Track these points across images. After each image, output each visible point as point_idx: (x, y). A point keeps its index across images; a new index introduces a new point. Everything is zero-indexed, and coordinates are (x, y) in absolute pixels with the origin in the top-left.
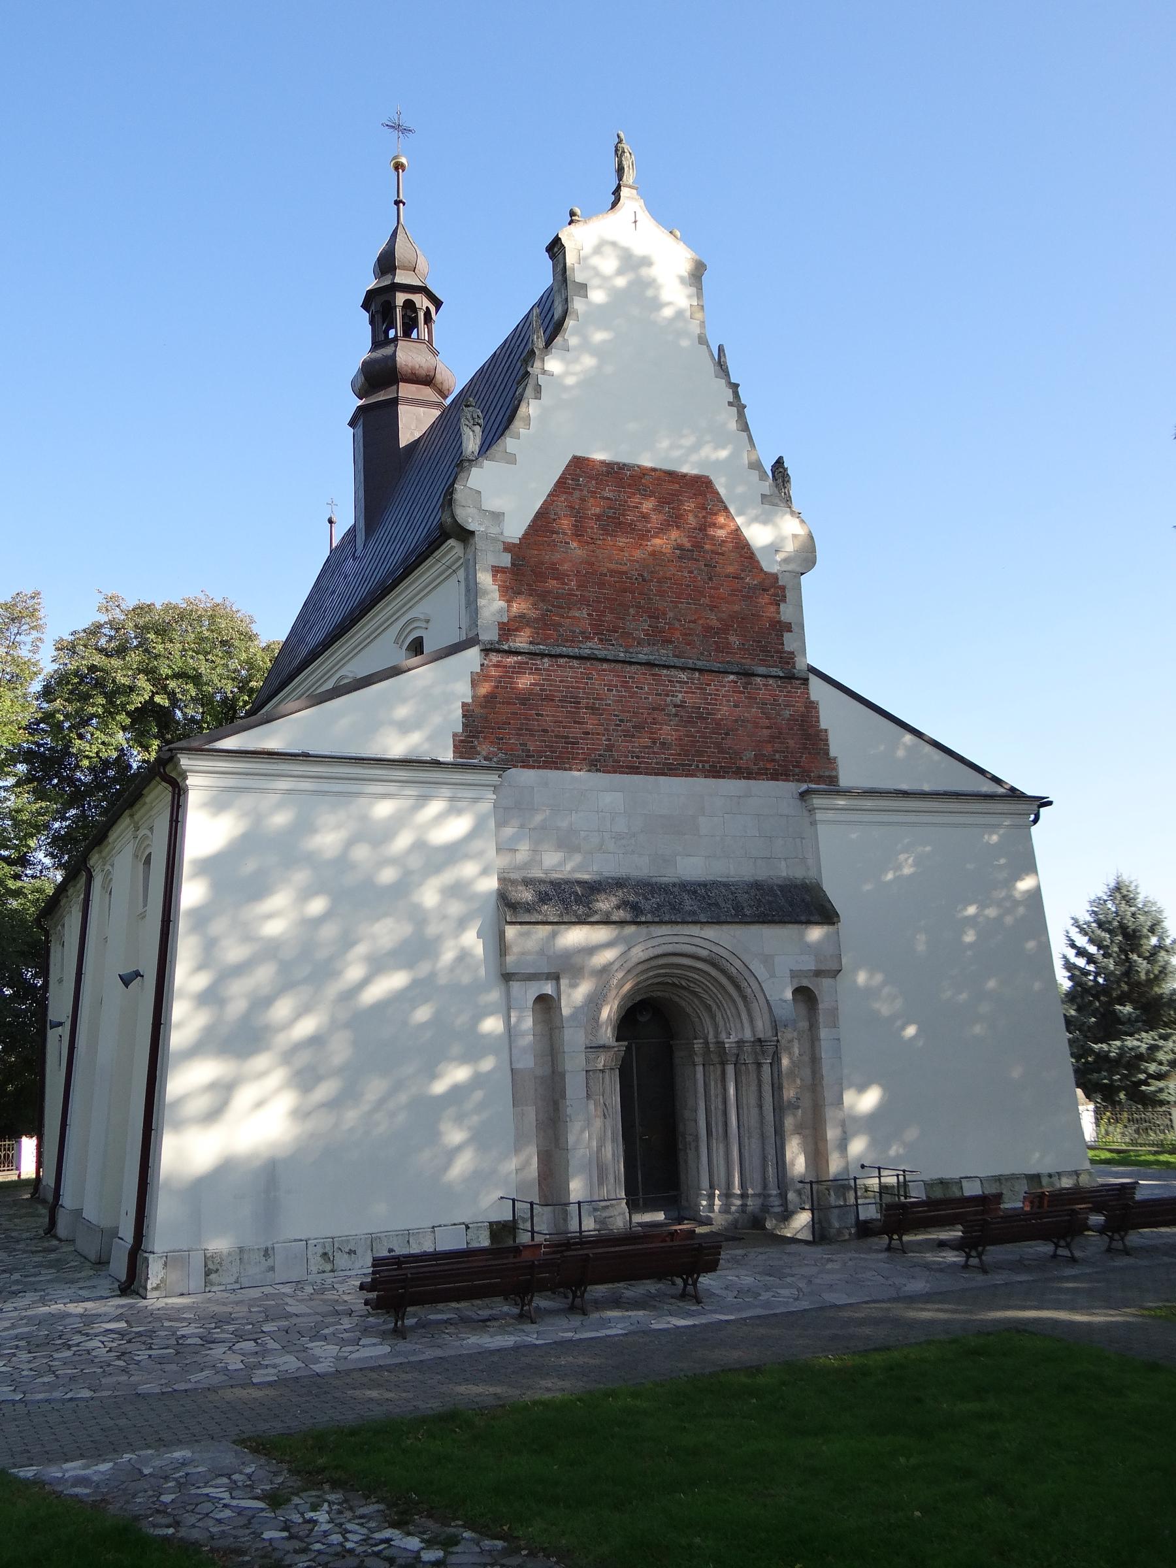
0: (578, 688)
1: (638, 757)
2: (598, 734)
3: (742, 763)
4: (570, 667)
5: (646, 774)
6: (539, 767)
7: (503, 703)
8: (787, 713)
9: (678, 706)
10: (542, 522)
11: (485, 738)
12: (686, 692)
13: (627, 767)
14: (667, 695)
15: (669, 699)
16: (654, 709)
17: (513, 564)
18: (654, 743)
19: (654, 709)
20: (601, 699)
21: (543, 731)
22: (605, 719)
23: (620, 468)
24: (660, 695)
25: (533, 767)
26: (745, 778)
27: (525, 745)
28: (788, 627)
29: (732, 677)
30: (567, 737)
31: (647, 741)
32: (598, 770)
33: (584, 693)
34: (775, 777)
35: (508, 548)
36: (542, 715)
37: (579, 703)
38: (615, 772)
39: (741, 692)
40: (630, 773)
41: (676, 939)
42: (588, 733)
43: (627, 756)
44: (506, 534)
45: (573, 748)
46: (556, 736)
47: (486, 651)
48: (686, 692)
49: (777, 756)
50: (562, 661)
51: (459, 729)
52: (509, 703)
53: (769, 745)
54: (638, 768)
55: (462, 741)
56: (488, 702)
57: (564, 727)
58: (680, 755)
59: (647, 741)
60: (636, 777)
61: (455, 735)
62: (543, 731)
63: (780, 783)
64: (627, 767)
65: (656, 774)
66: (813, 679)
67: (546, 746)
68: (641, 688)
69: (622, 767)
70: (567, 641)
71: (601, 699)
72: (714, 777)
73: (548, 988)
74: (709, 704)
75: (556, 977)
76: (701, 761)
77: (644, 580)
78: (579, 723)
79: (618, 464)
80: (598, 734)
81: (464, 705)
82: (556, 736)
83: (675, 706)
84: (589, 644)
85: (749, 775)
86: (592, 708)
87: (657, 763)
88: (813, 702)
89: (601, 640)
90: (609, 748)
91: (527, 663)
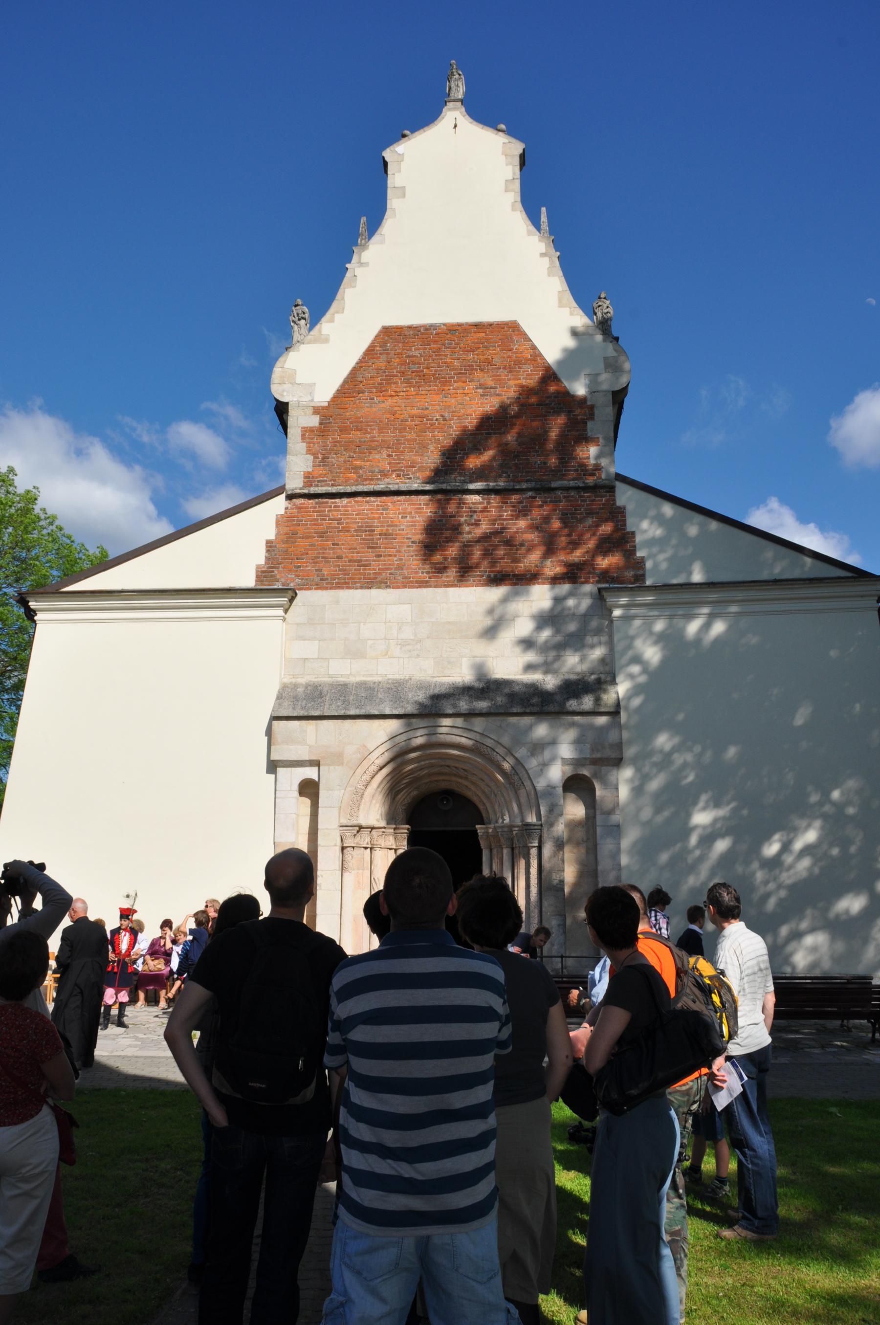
0: (374, 518)
2: (390, 556)
4: (368, 502)
5: (436, 586)
6: (331, 588)
7: (303, 538)
10: (351, 387)
11: (284, 568)
13: (416, 582)
17: (321, 424)
20: (396, 526)
21: (338, 557)
22: (398, 543)
23: (427, 329)
25: (326, 588)
27: (320, 570)
29: (530, 494)
30: (359, 561)
32: (388, 587)
33: (379, 522)
35: (317, 410)
36: (337, 544)
37: (374, 531)
38: (405, 587)
40: (420, 587)
42: (380, 556)
43: (417, 573)
44: (315, 400)
45: (364, 570)
46: (350, 561)
47: (290, 497)
50: (359, 499)
51: (262, 561)
52: (308, 537)
54: (427, 582)
55: (263, 572)
56: (290, 538)
57: (358, 552)
61: (258, 567)
62: (338, 557)
64: (416, 582)
65: (445, 586)
66: (620, 486)
67: (340, 570)
69: (412, 582)
70: (366, 480)
71: (396, 526)
73: (311, 773)
75: (317, 764)
77: (445, 420)
78: (372, 548)
79: (424, 326)
80: (390, 556)
81: (268, 542)
82: (350, 561)
84: (387, 480)
86: (386, 534)
88: (619, 508)
89: (398, 476)
90: (400, 567)
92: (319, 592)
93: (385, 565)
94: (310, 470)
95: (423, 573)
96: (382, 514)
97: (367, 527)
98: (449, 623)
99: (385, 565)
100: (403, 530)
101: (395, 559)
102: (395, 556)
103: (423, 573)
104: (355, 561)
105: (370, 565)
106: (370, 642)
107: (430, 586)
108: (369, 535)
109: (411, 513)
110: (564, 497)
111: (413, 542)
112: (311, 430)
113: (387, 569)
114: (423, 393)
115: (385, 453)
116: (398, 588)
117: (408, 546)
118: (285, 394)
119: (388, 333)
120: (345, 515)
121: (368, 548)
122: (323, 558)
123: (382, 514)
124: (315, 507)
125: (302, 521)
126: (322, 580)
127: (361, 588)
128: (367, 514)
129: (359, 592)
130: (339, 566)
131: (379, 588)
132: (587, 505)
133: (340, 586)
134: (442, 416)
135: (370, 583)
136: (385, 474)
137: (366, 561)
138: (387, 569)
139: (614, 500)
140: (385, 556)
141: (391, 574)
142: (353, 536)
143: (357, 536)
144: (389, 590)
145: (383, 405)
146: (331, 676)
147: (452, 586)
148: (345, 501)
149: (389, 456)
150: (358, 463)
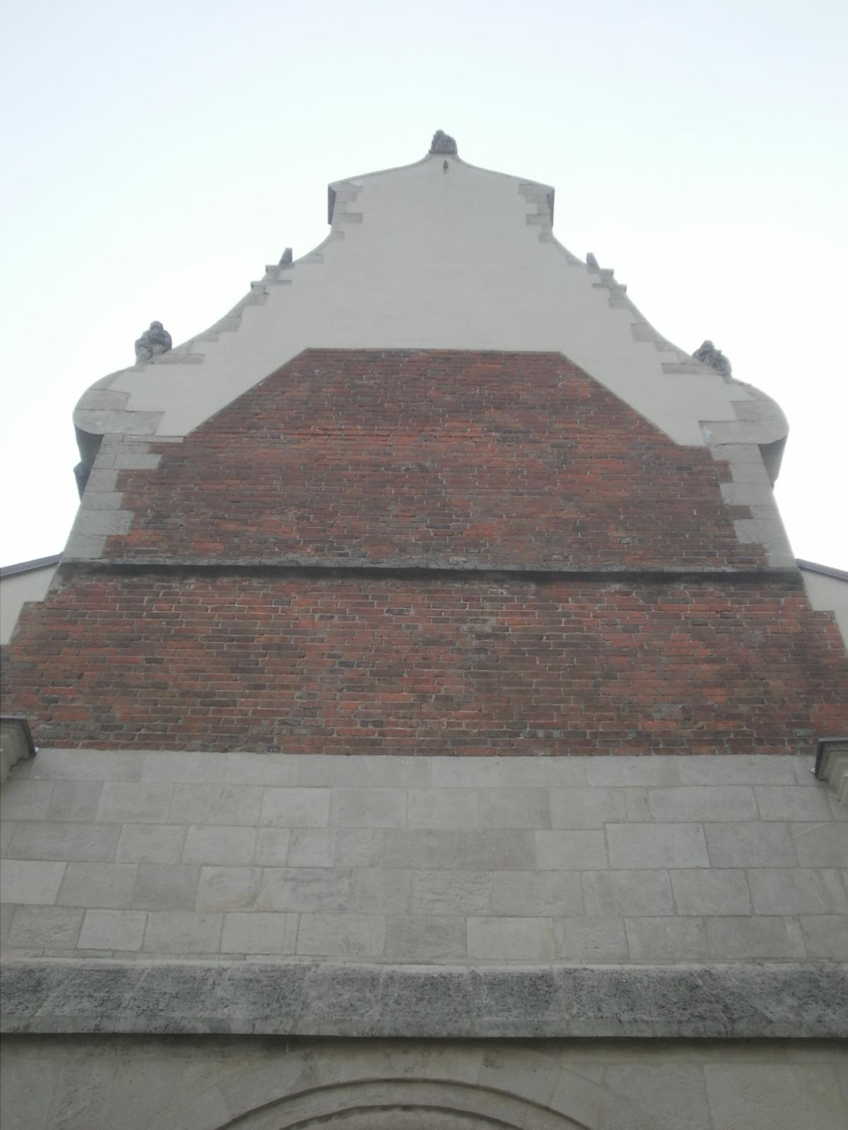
0: (254, 617)
1: (378, 724)
3: (653, 727)
4: (243, 589)
8: (758, 636)
9: (487, 636)
12: (506, 614)
13: (348, 741)
14: (463, 621)
15: (464, 627)
16: (428, 643)
18: (423, 697)
19: (428, 643)
24: (446, 621)
25: (115, 747)
26: (658, 752)
28: (744, 513)
31: (406, 697)
34: (741, 745)
36: (160, 661)
39: (640, 608)
40: (357, 752)
41: (400, 1095)
42: (264, 687)
48: (506, 614)
49: (743, 709)
50: (225, 581)
53: (719, 691)
54: (374, 743)
58: (488, 716)
59: (406, 697)
60: (368, 759)
63: (757, 758)
64: (348, 741)
68: (401, 612)
69: (337, 742)
72: (576, 753)
74: (563, 630)
76: (541, 726)
78: (243, 670)
82: (184, 694)
83: (480, 636)
85: (667, 745)
86: (279, 647)
87: (427, 733)
91: (151, 587)
92: (94, 754)
93: (270, 704)
94: (122, 533)
95: (364, 724)
96: (276, 610)
97: (235, 632)
98: (430, 832)
99: (270, 704)
100: (322, 640)
101: (298, 693)
102: (298, 688)
103: (364, 724)
104: (196, 695)
105: (234, 703)
106: (208, 872)
107: (383, 752)
108: (240, 647)
109: (344, 612)
110: (694, 595)
111: (342, 664)
112: (141, 475)
113: (274, 713)
114: (380, 433)
115: (291, 515)
116: (301, 752)
117: (331, 671)
118: (99, 424)
119: (313, 360)
120: (186, 608)
121: (234, 670)
122: (117, 684)
123: (276, 610)
124: (120, 593)
125: (84, 615)
126: (104, 728)
127: (204, 748)
128: (239, 610)
129: (197, 757)
130: (156, 703)
131: (249, 750)
132: (748, 610)
133: (149, 742)
134: (419, 465)
135: (225, 739)
136: (289, 546)
137: (225, 695)
138: (274, 713)
139: (806, 602)
140: (272, 688)
141: (283, 723)
142: (201, 647)
143: (209, 647)
144: (274, 756)
145: (297, 446)
146: (82, 953)
147: (440, 752)
148: (192, 583)
149: (300, 518)
150: (232, 527)
